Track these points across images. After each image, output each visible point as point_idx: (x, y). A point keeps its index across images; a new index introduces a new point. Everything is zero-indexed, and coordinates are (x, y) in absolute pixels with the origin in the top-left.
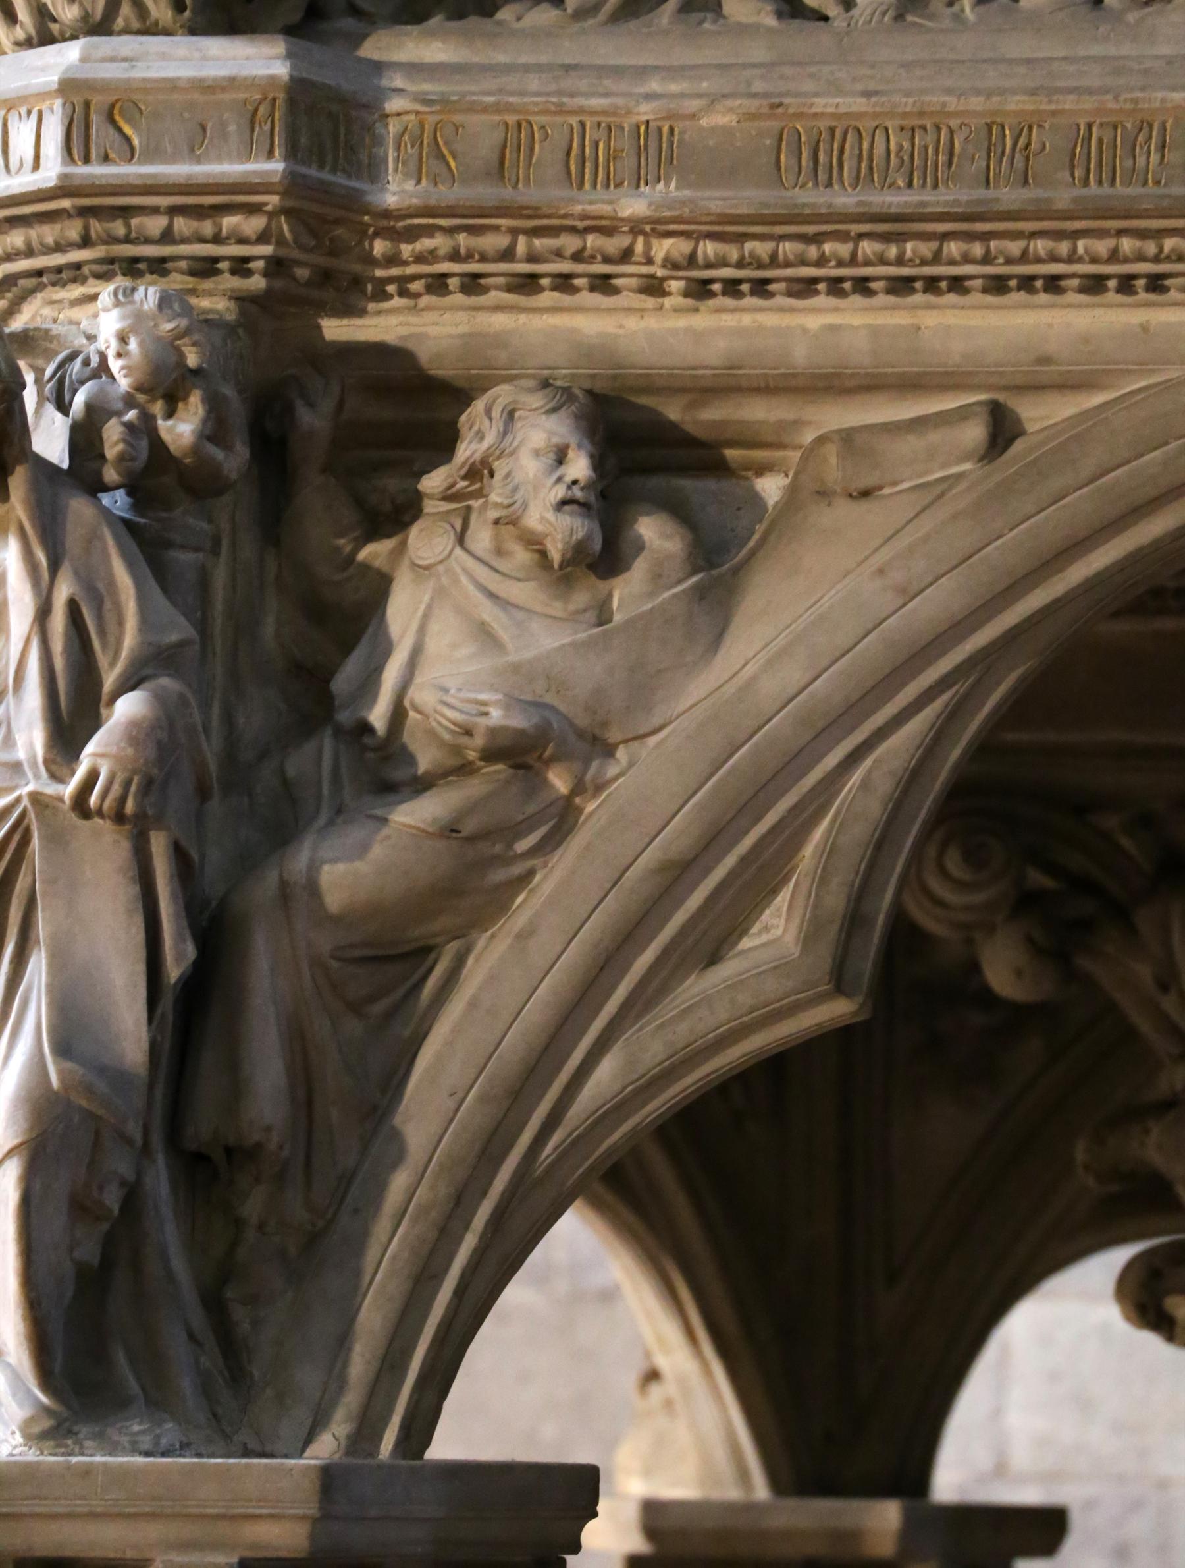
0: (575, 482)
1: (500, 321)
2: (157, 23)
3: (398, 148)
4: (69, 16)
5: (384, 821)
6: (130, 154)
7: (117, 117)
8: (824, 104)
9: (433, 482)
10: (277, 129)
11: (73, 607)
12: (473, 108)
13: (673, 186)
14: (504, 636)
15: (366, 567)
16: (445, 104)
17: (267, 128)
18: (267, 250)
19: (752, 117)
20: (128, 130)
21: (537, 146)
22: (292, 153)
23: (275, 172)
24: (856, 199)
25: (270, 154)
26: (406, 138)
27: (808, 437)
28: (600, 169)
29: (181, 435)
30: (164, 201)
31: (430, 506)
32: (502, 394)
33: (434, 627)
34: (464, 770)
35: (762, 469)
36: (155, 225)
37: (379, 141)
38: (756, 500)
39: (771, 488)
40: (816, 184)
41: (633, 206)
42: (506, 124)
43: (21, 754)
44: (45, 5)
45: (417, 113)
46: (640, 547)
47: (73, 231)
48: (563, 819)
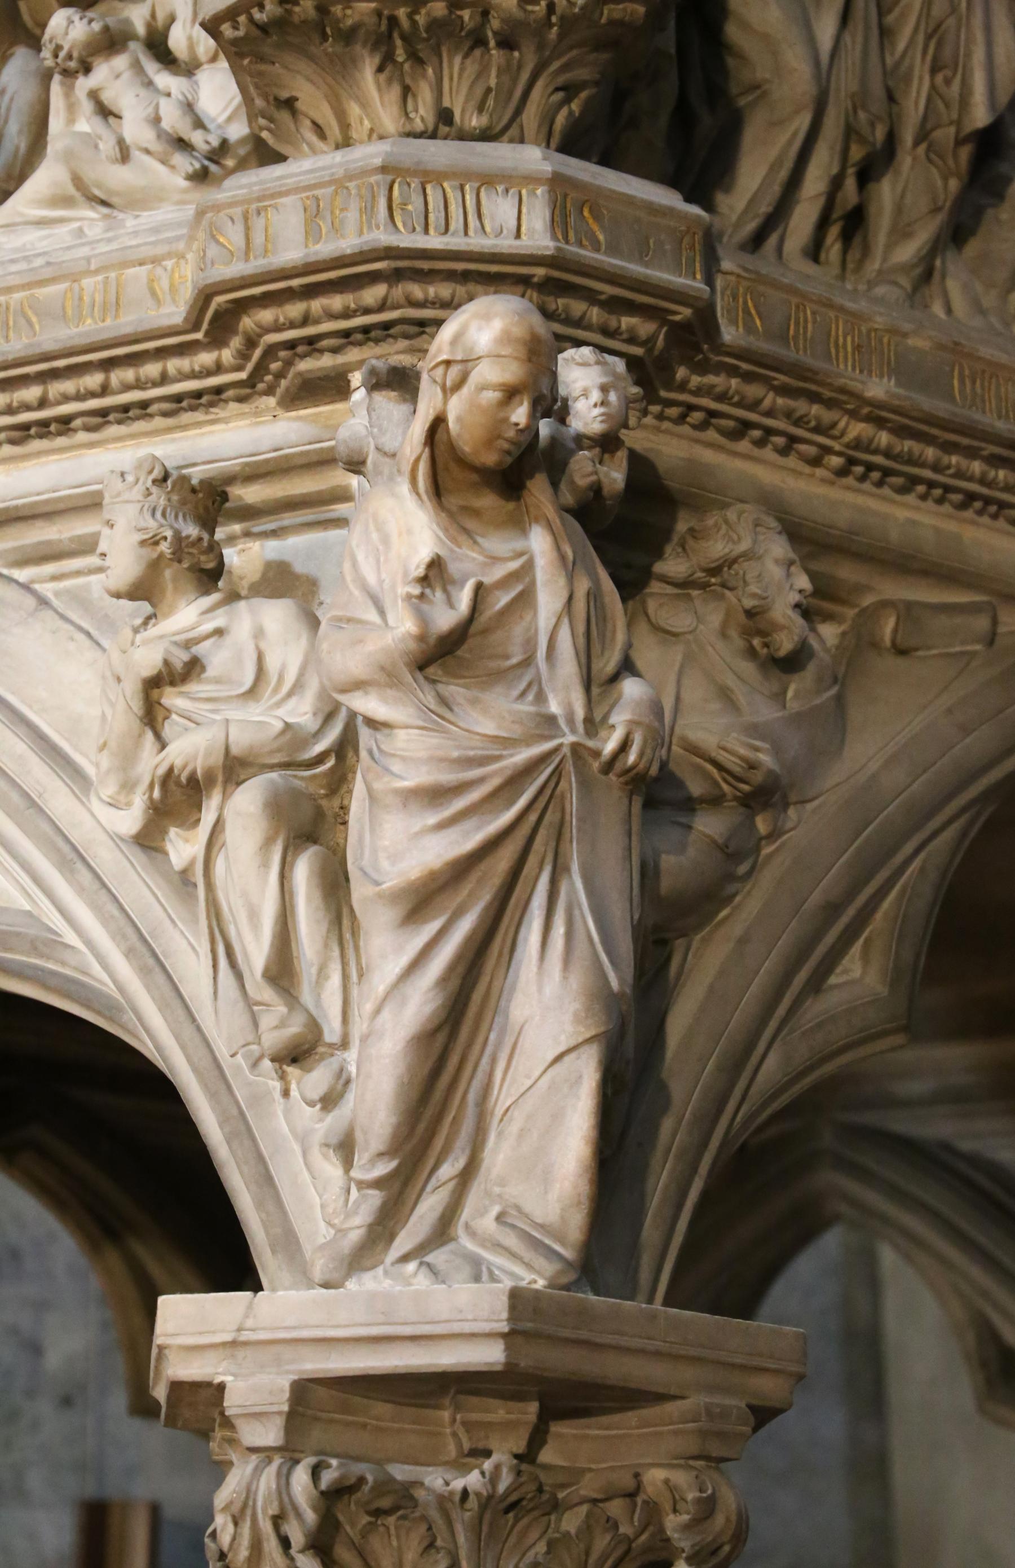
0: (800, 591)
1: (708, 456)
3: (723, 299)
4: (474, 122)
14: (742, 700)
21: (810, 326)
29: (615, 480)
30: (609, 290)
33: (686, 682)
43: (554, 707)
45: (739, 276)
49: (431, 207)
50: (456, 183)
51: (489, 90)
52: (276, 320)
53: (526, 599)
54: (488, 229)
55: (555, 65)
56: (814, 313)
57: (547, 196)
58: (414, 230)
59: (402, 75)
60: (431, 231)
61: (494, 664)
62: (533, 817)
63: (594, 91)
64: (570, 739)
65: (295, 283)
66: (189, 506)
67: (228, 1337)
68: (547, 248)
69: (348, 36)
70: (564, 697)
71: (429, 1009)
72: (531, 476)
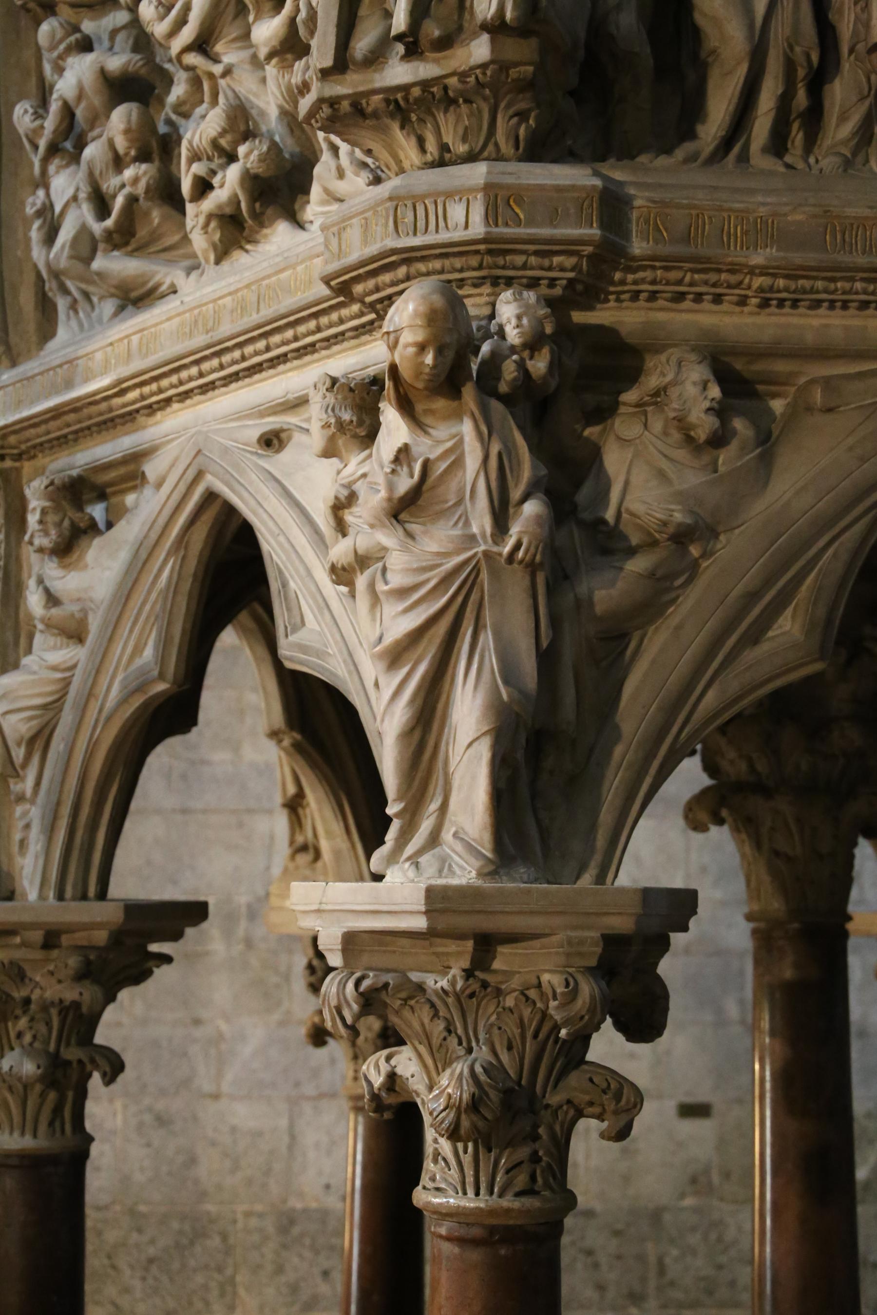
3: (638, 225)
4: (461, 149)
5: (621, 569)
6: (518, 223)
7: (512, 203)
8: (850, 211)
9: (630, 396)
10: (595, 213)
11: (500, 455)
12: (679, 206)
13: (774, 250)
15: (587, 439)
16: (663, 204)
18: (571, 275)
19: (815, 216)
20: (518, 210)
22: (602, 226)
23: (596, 234)
24: (866, 260)
25: (591, 226)
26: (642, 219)
27: (802, 380)
28: (739, 240)
29: (539, 369)
30: (532, 248)
31: (622, 409)
32: (675, 353)
34: (654, 544)
35: (774, 396)
37: (629, 221)
38: (770, 412)
39: (778, 405)
40: (845, 252)
41: (757, 259)
42: (691, 215)
43: (475, 529)
44: (447, 144)
45: (648, 207)
46: (734, 433)
48: (694, 569)
50: (433, 200)
51: (466, 128)
53: (458, 463)
54: (450, 226)
55: (502, 105)
56: (710, 218)
58: (408, 234)
59: (414, 129)
60: (418, 234)
61: (437, 508)
62: (460, 599)
63: (537, 111)
64: (483, 548)
65: (361, 271)
66: (349, 400)
67: (315, 907)
68: (480, 234)
69: (375, 115)
70: (481, 521)
71: (404, 719)
72: (463, 385)
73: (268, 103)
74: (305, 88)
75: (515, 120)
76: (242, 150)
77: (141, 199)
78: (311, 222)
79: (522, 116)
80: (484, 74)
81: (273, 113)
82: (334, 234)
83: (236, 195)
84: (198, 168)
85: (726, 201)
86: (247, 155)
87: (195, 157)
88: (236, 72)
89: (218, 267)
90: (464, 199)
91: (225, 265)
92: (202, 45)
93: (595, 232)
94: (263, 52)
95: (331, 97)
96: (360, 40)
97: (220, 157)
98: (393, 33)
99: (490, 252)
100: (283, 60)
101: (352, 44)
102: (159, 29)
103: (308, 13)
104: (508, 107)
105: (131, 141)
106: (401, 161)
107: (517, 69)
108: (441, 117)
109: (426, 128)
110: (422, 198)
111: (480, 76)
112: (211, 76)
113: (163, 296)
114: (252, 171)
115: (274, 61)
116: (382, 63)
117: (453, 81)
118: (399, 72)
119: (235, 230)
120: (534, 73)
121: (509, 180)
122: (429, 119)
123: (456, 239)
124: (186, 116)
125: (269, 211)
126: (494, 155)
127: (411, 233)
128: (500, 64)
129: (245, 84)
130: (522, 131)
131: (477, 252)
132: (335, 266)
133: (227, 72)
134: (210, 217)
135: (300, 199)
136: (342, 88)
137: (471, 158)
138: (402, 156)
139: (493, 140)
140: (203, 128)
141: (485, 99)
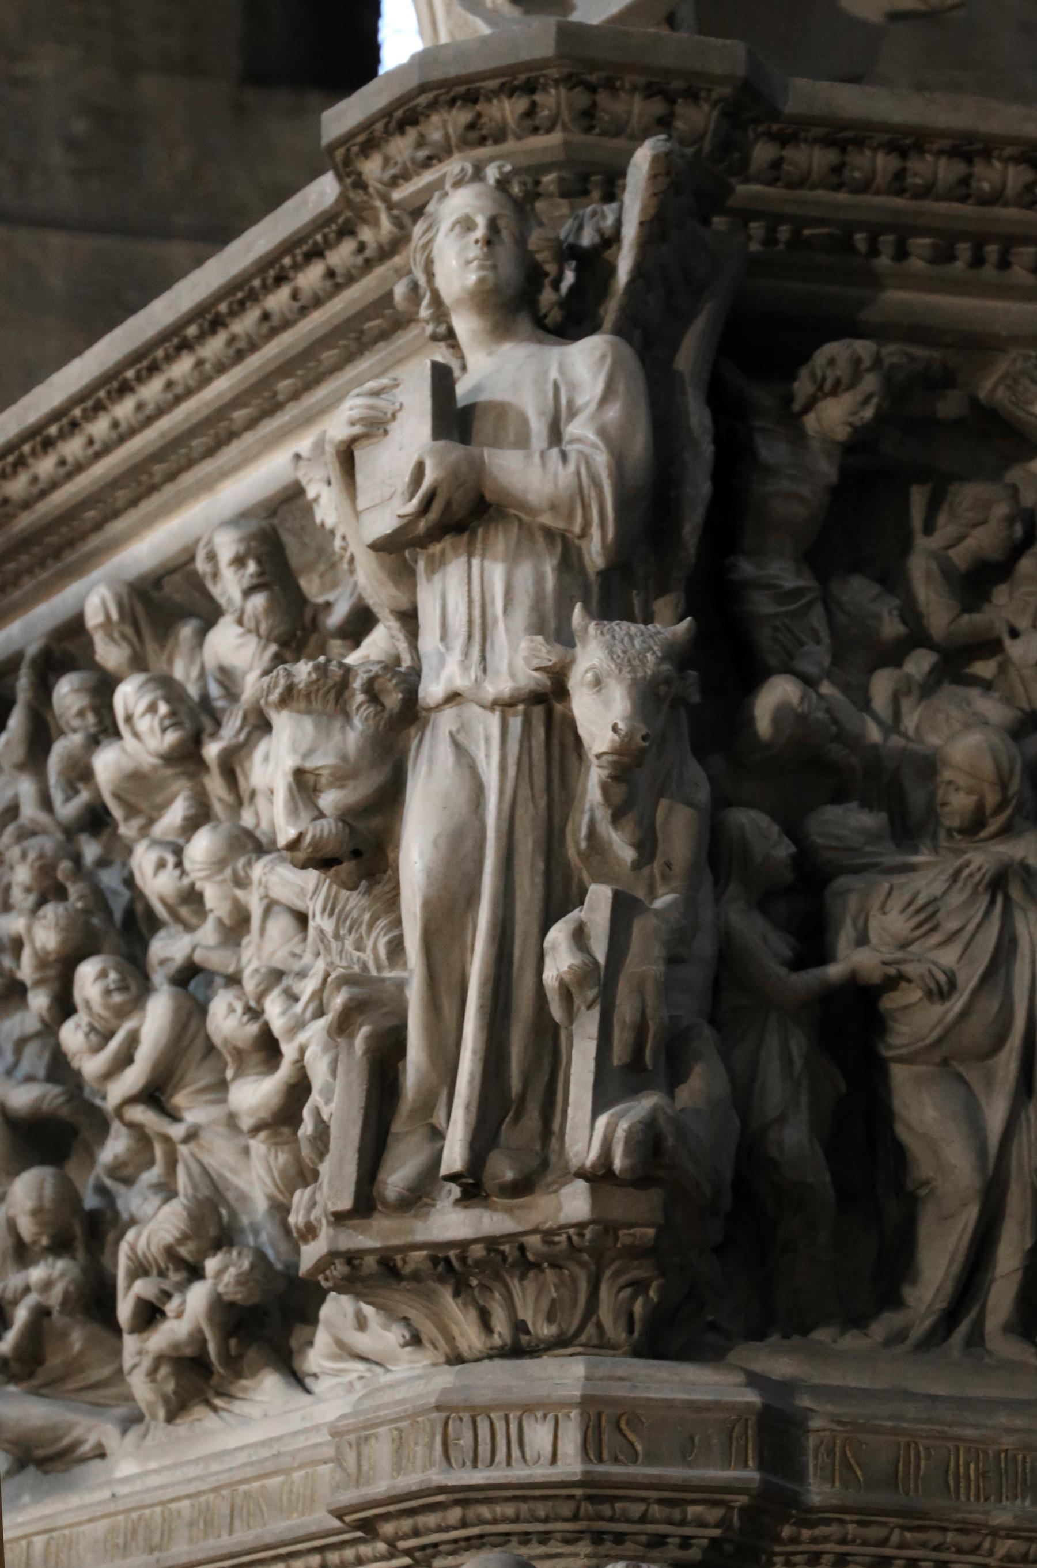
2: (609, 1340)
4: (546, 1332)
7: (623, 1426)
17: (742, 1442)
18: (716, 1532)
20: (632, 1437)
23: (752, 1480)
25: (746, 1465)
36: (636, 1510)
44: (524, 1322)
47: (567, 1509)
49: (480, 1439)
50: (501, 1414)
51: (553, 1302)
52: (396, 1533)
55: (608, 1273)
57: (579, 1418)
58: (464, 1464)
59: (473, 1297)
60: (480, 1465)
68: (574, 1474)
69: (416, 1277)
73: (251, 1183)
74: (310, 1232)
75: (627, 1292)
76: (211, 1265)
77: (55, 1314)
78: (315, 1376)
79: (639, 1286)
80: (581, 1235)
81: (261, 1205)
82: (350, 1445)
83: (200, 1331)
84: (143, 1288)
85: (951, 1425)
86: (219, 1273)
87: (140, 1270)
88: (205, 1137)
89: (170, 1428)
90: (551, 1415)
91: (182, 1428)
92: (155, 1095)
93: (751, 1475)
94: (246, 1123)
95: (349, 1251)
96: (394, 1170)
97: (177, 1270)
98: (444, 1171)
99: (589, 1498)
100: (276, 1134)
101: (382, 1176)
102: (91, 1066)
103: (316, 1127)
104: (617, 1274)
105: (42, 1225)
106: (454, 1338)
107: (631, 1231)
108: (515, 1285)
109: (493, 1299)
110: (486, 1410)
111: (575, 1238)
112: (167, 1139)
113: (84, 1459)
114: (226, 1298)
115: (263, 1135)
116: (427, 1205)
117: (534, 1241)
118: (451, 1222)
119: (198, 1380)
120: (657, 1237)
121: (619, 1390)
122: (497, 1286)
123: (539, 1480)
124: (129, 1181)
125: (252, 1354)
126: (595, 1341)
127: (468, 1463)
128: (605, 1226)
129: (218, 1153)
130: (638, 1307)
131: (571, 1497)
132: (348, 1497)
133: (192, 1136)
134: (159, 1360)
135: (299, 1333)
136: (364, 1239)
137: (560, 1343)
138: (455, 1331)
139: (594, 1319)
140: (155, 1224)
141: (583, 1265)
